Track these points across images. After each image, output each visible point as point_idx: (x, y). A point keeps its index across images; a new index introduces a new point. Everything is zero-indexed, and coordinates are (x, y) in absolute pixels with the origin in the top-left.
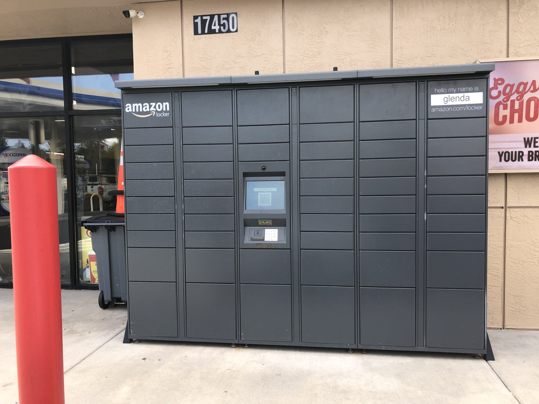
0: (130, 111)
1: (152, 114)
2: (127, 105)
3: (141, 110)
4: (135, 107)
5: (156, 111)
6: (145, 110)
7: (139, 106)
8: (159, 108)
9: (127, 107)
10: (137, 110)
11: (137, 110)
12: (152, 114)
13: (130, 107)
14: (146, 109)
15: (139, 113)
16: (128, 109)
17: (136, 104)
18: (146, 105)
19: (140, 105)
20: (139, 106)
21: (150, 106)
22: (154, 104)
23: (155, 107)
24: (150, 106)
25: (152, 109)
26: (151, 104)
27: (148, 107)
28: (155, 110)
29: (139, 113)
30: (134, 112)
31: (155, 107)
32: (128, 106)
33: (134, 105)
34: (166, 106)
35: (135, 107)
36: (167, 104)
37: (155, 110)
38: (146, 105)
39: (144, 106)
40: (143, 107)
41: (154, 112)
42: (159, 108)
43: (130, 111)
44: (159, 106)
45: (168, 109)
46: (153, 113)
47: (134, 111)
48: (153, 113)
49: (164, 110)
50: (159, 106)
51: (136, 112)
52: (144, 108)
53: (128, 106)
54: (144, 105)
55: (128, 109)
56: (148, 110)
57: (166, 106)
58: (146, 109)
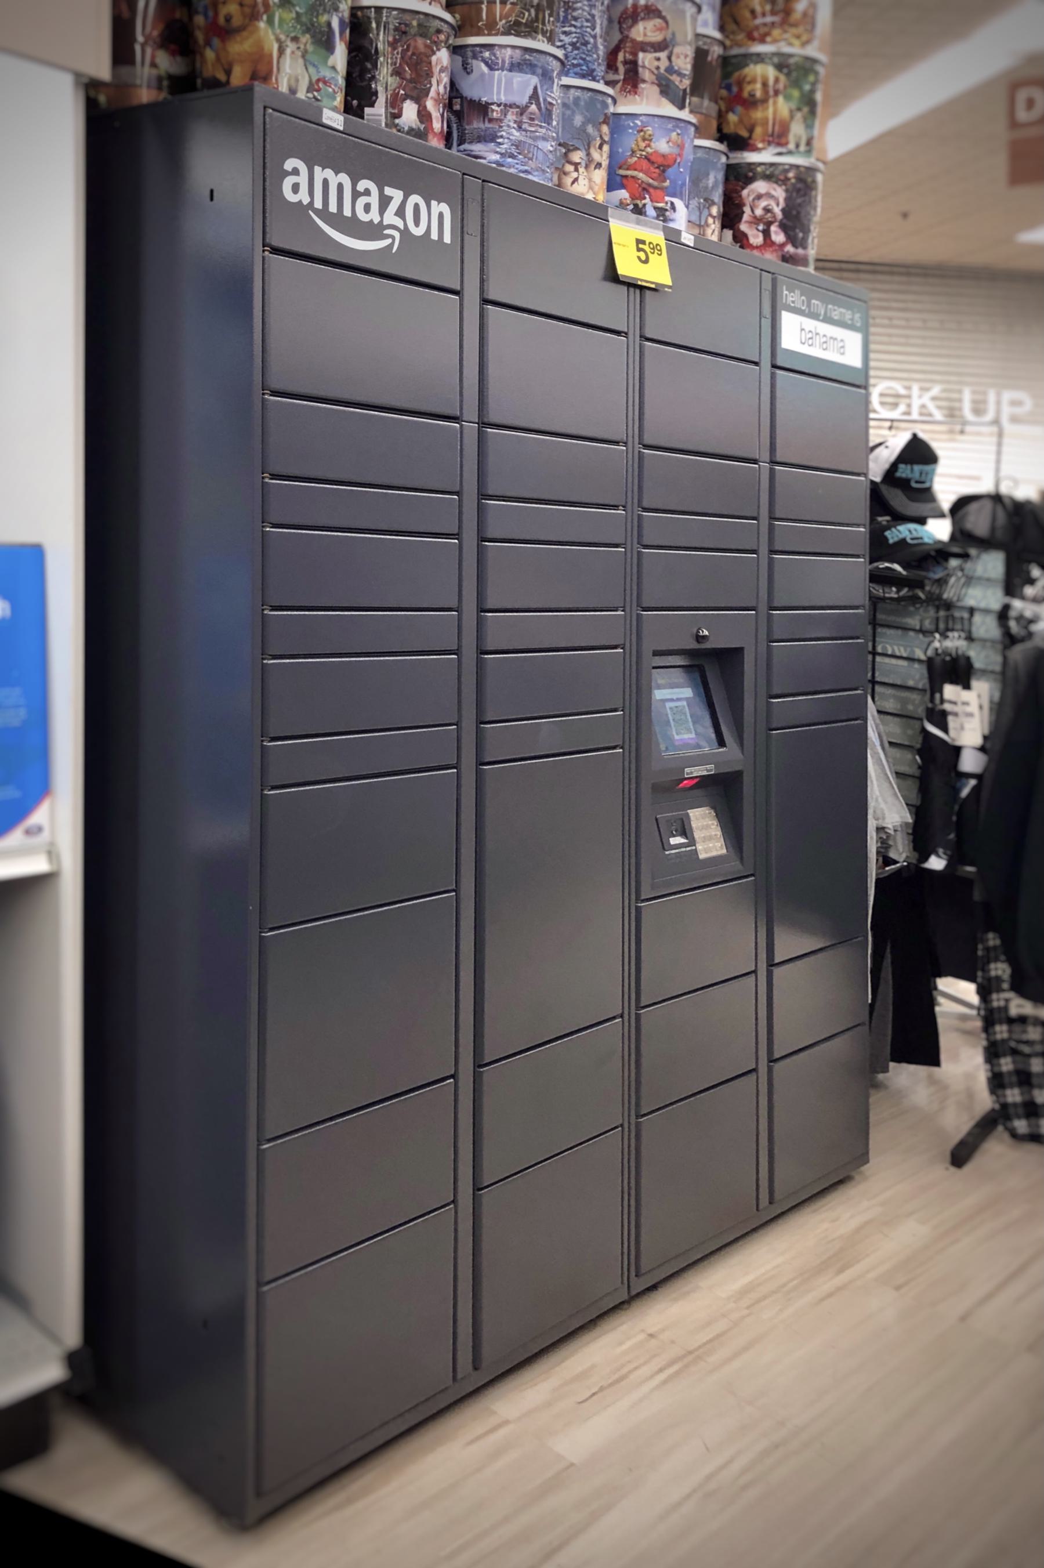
0: (300, 201)
1: (389, 241)
2: (290, 164)
3: (347, 212)
5: (405, 233)
9: (288, 174)
10: (333, 208)
11: (333, 208)
12: (389, 241)
13: (303, 179)
15: (338, 221)
16: (296, 188)
17: (329, 173)
19: (344, 179)
21: (384, 202)
24: (384, 202)
26: (388, 191)
27: (374, 200)
28: (400, 224)
29: (338, 221)
30: (317, 212)
31: (400, 213)
32: (296, 172)
33: (320, 174)
34: (441, 216)
35: (326, 183)
36: (445, 208)
37: (400, 224)
40: (356, 195)
41: (397, 235)
43: (300, 201)
45: (447, 239)
46: (393, 238)
47: (318, 204)
49: (434, 236)
51: (324, 214)
52: (361, 201)
53: (296, 172)
54: (362, 185)
55: (296, 188)
56: (374, 216)
57: (441, 216)
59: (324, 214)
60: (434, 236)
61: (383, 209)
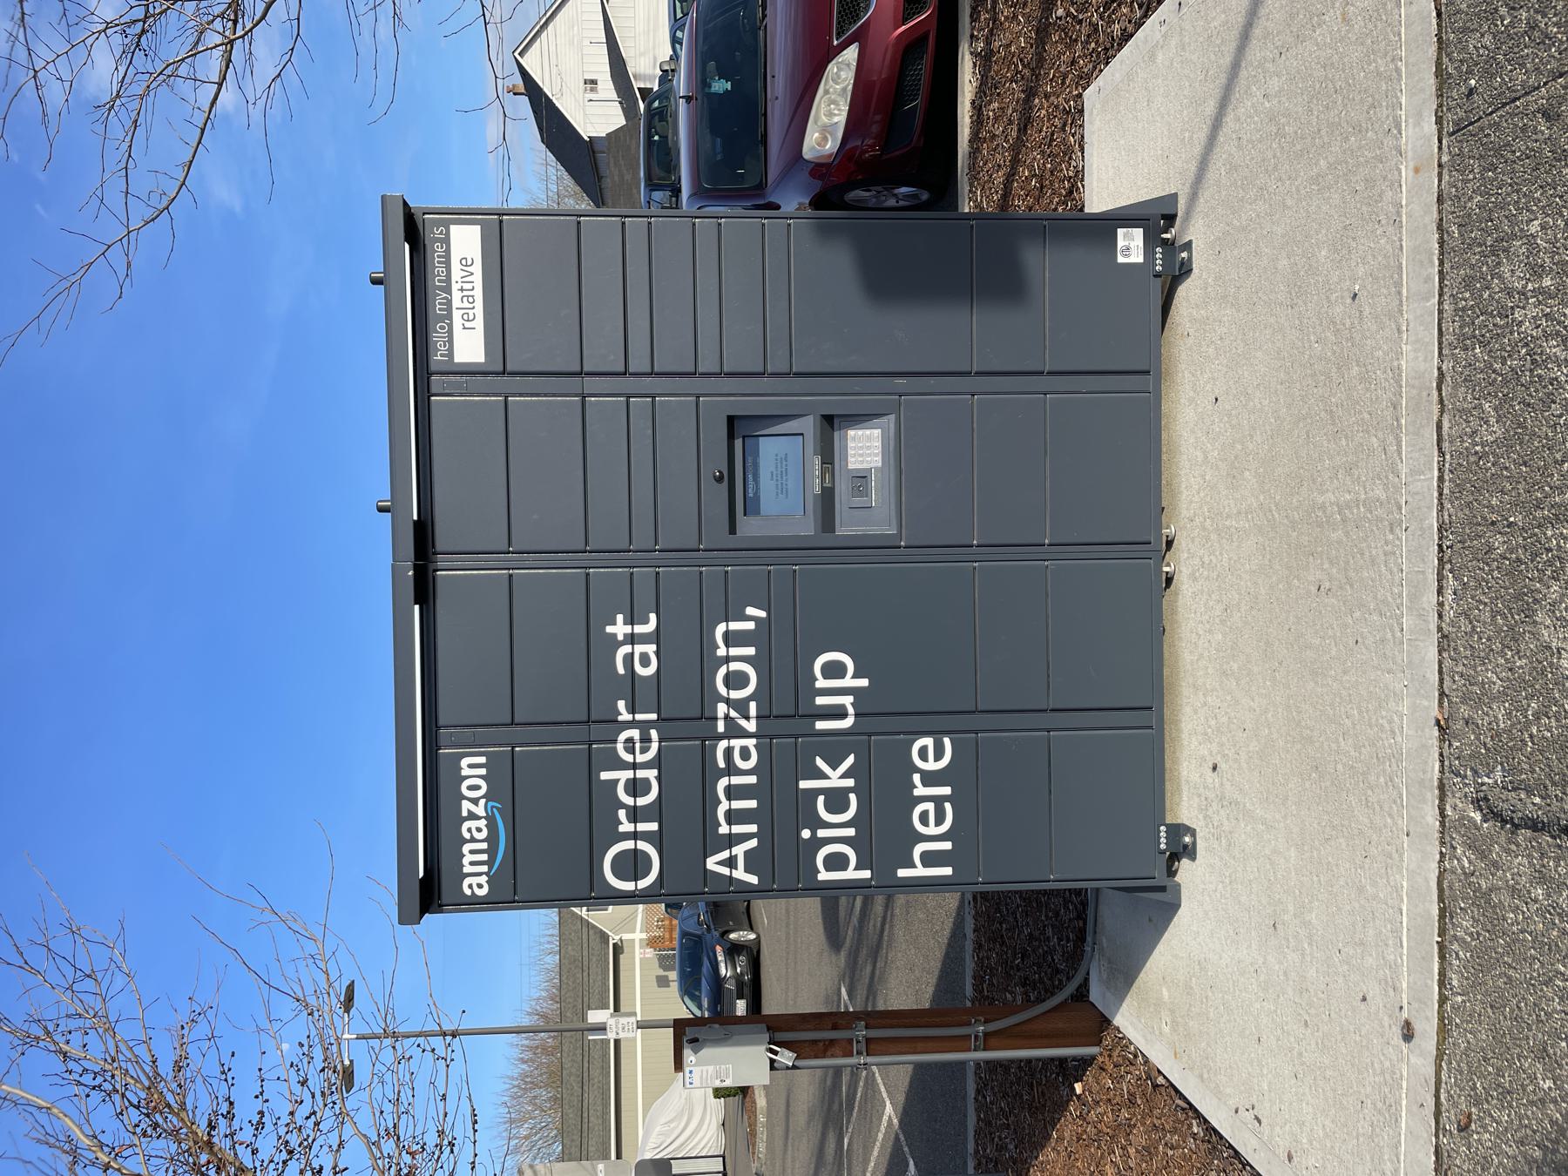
1: (494, 809)
2: (468, 892)
3: (484, 846)
4: (472, 863)
6: (484, 834)
7: (472, 852)
8: (477, 788)
9: (473, 892)
10: (484, 857)
12: (494, 809)
13: (474, 880)
14: (479, 830)
15: (492, 851)
17: (466, 861)
18: (469, 830)
19: (466, 848)
20: (472, 852)
21: (472, 816)
22: (466, 805)
23: (475, 801)
24: (472, 816)
25: (480, 810)
26: (465, 814)
28: (483, 801)
31: (475, 801)
32: (470, 886)
33: (467, 869)
34: (471, 766)
35: (472, 863)
37: (483, 801)
38: (469, 830)
39: (472, 836)
40: (473, 840)
41: (490, 804)
42: (477, 788)
44: (472, 788)
46: (492, 807)
47: (485, 868)
48: (492, 807)
49: (483, 771)
50: (472, 788)
54: (467, 836)
55: (480, 886)
56: (482, 823)
57: (471, 766)
58: (479, 830)
59: (490, 863)
60: (483, 771)
61: (478, 818)
